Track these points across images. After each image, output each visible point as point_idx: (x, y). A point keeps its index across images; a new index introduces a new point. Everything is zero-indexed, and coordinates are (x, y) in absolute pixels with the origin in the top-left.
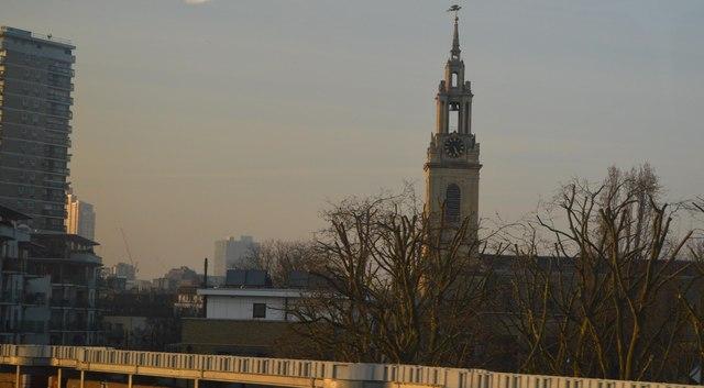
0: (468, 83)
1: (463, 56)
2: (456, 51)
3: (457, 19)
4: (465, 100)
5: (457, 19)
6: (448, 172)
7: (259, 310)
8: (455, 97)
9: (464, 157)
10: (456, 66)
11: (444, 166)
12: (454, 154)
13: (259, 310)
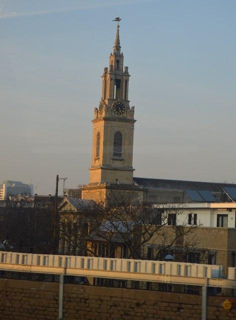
0: (127, 68)
1: (122, 50)
2: (118, 47)
3: (118, 27)
4: (125, 78)
5: (118, 27)
6: (114, 123)
7: (221, 218)
8: (118, 78)
9: (125, 115)
10: (118, 57)
11: (114, 120)
12: (117, 112)
13: (221, 218)
